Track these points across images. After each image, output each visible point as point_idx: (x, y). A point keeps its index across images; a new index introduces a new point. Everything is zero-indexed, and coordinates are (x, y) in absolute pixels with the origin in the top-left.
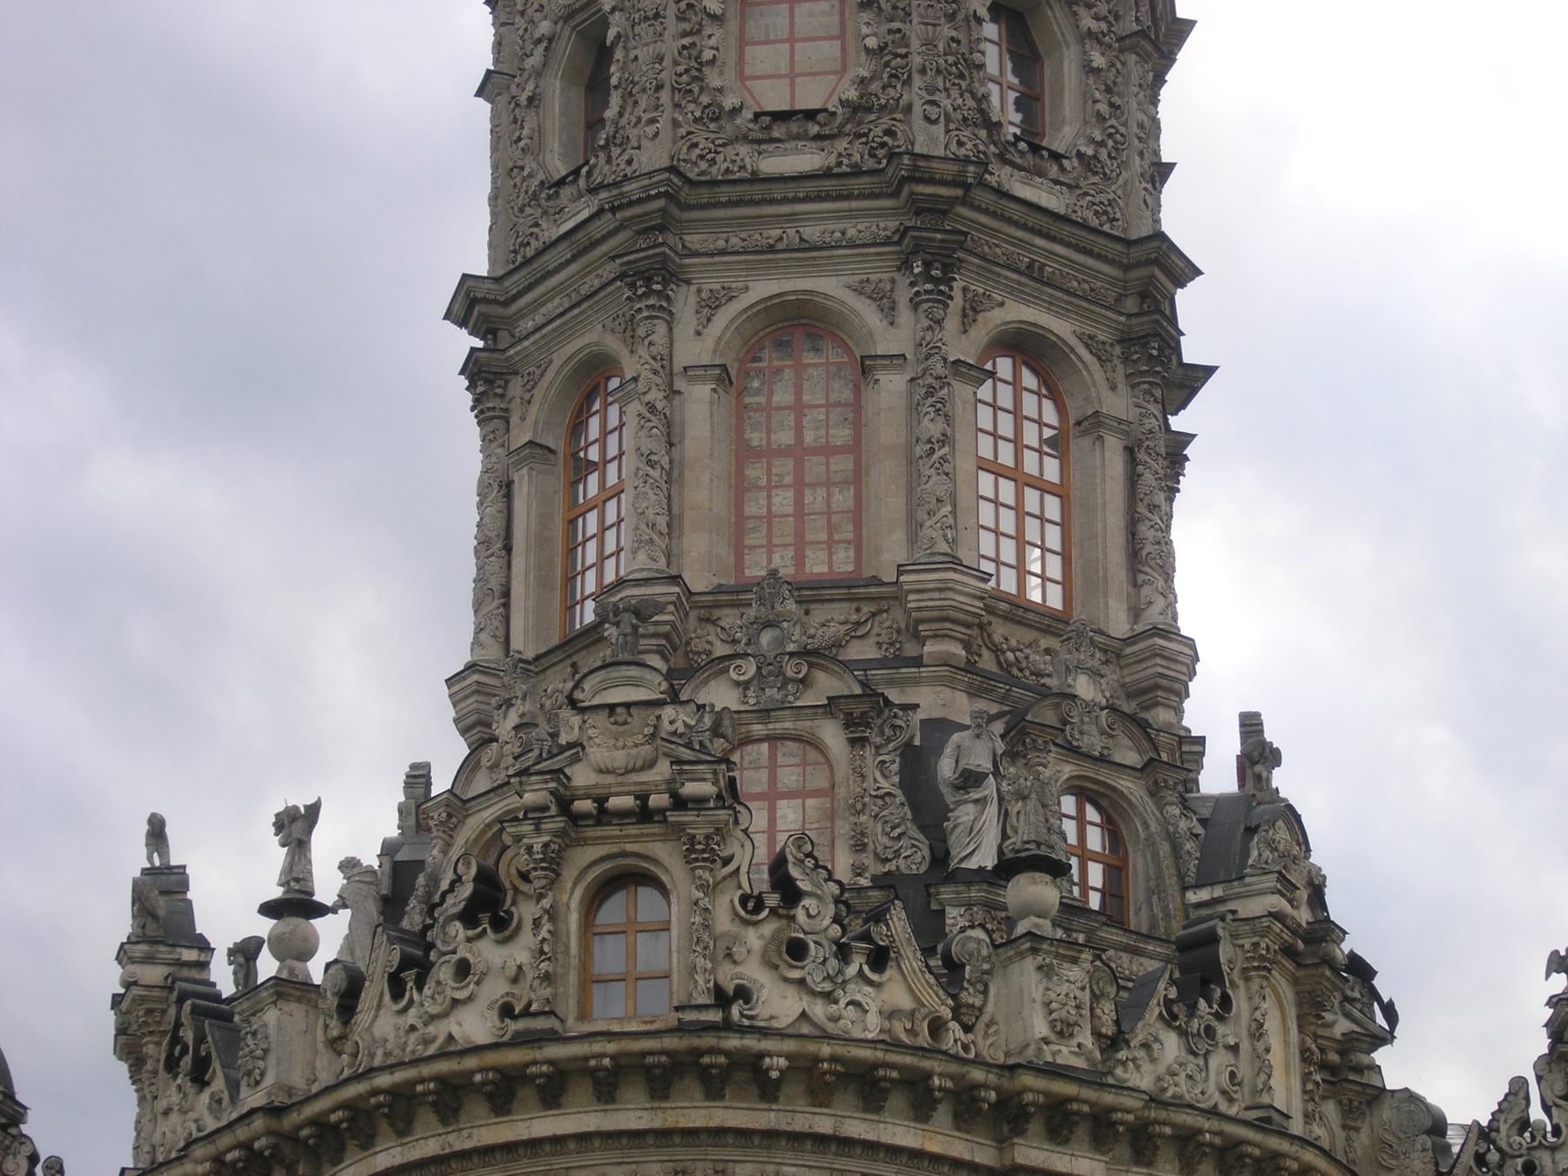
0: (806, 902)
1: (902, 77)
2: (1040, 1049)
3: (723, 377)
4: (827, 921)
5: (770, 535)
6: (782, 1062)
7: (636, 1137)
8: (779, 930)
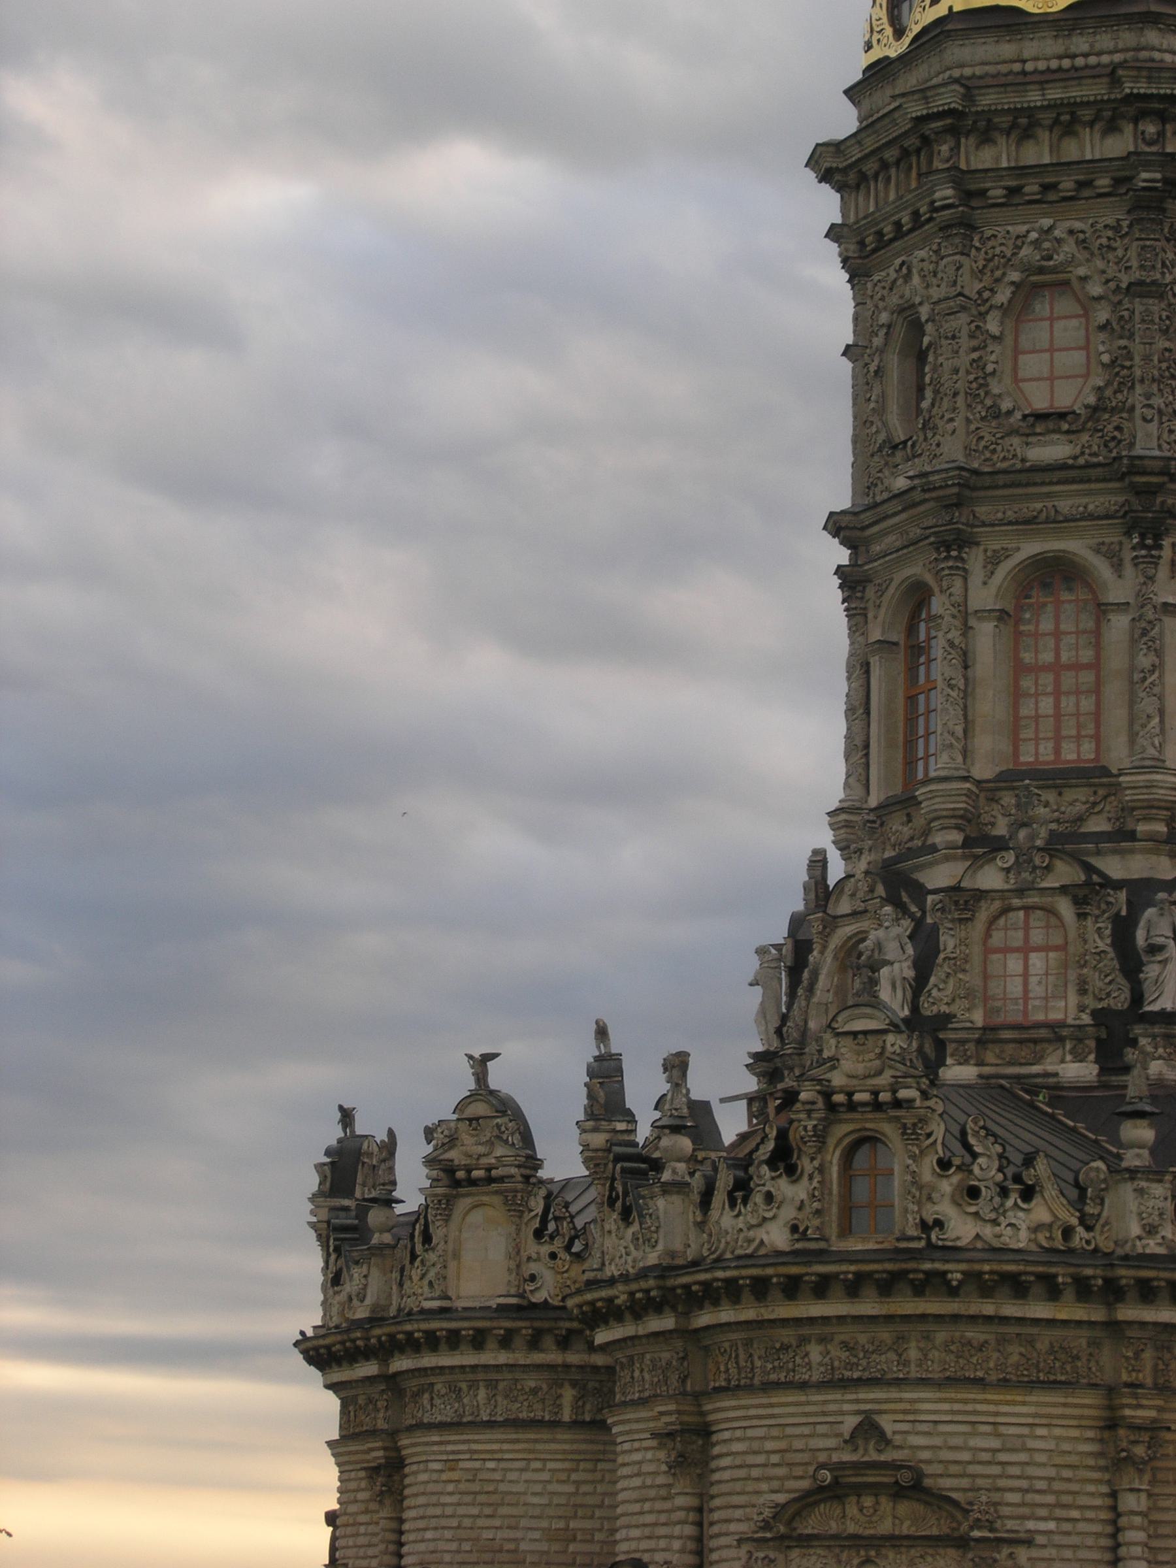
0: (980, 1160)
1: (1128, 384)
2: (1134, 1246)
3: (1003, 615)
4: (993, 1172)
5: (1037, 730)
6: (959, 1276)
7: (873, 1319)
8: (961, 1180)
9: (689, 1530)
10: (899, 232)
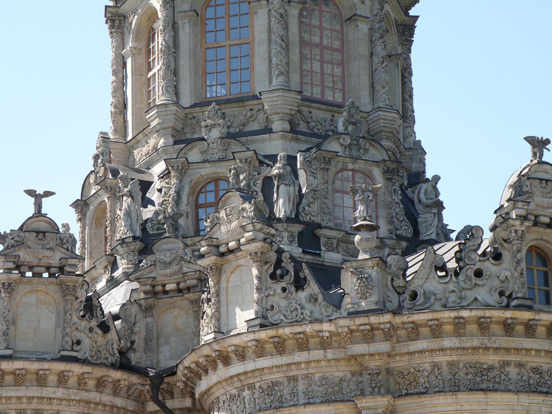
5: (312, 80)
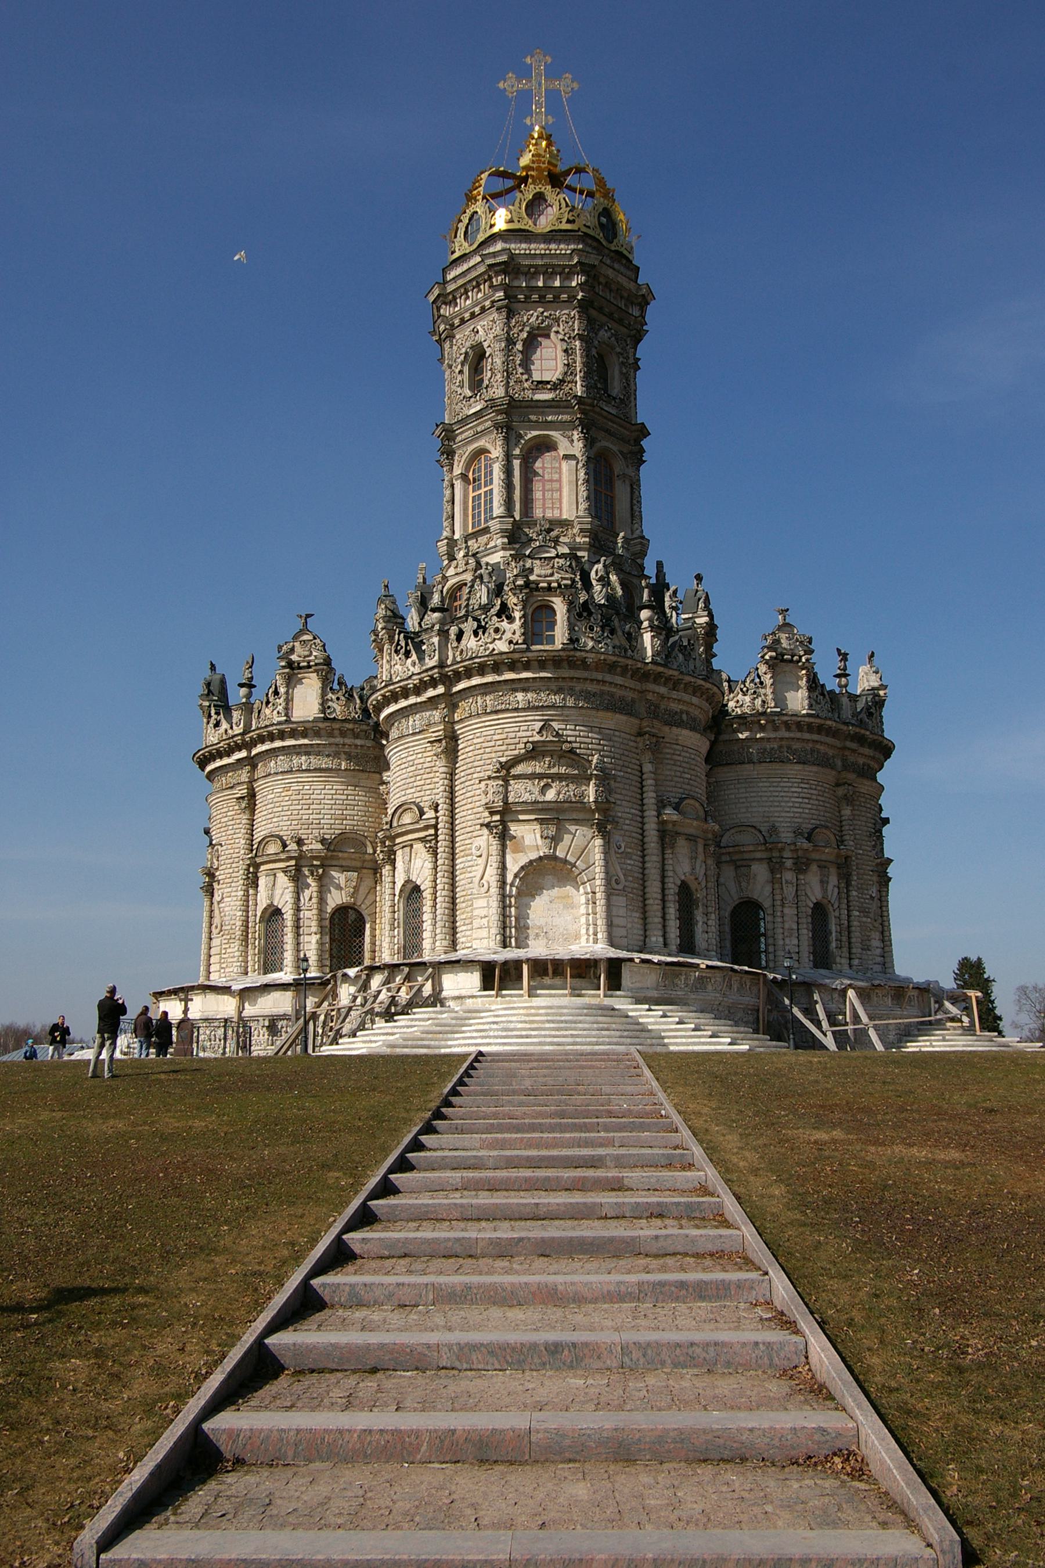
9: (446, 782)
10: (473, 316)
